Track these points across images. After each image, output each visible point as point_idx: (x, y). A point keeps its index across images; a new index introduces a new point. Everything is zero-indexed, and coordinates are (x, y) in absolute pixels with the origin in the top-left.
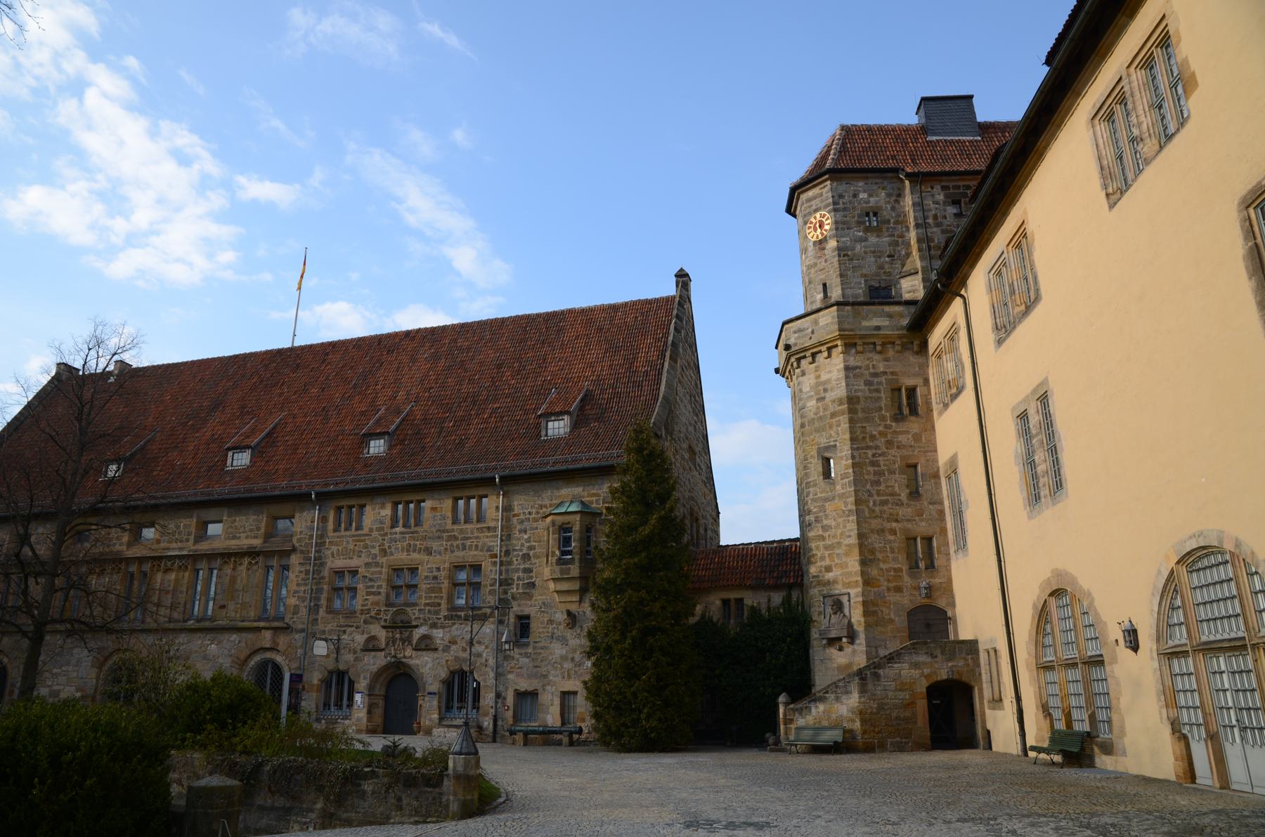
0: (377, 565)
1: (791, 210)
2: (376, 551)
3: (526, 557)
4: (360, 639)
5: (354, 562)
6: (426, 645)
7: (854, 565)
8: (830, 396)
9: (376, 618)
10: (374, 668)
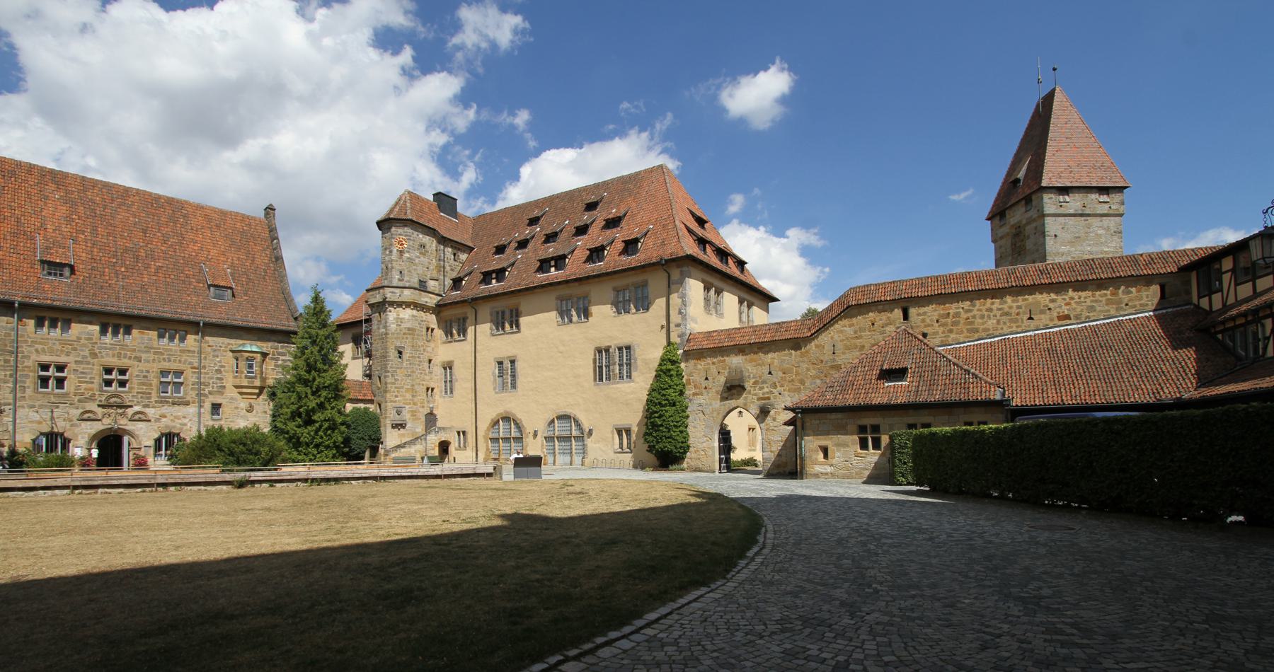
0: (88, 363)
1: (385, 224)
2: (87, 353)
3: (219, 371)
4: (76, 413)
5: (62, 359)
6: (141, 418)
7: (409, 396)
8: (404, 325)
9: (92, 398)
10: (93, 432)
